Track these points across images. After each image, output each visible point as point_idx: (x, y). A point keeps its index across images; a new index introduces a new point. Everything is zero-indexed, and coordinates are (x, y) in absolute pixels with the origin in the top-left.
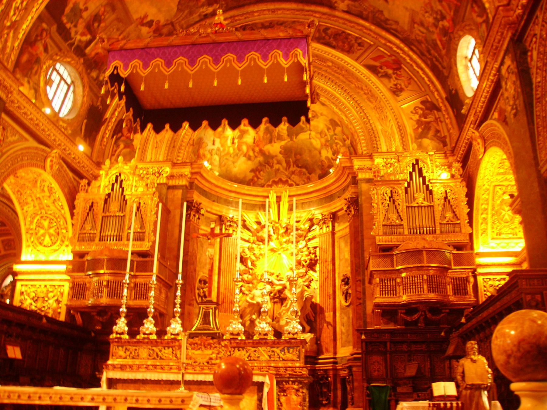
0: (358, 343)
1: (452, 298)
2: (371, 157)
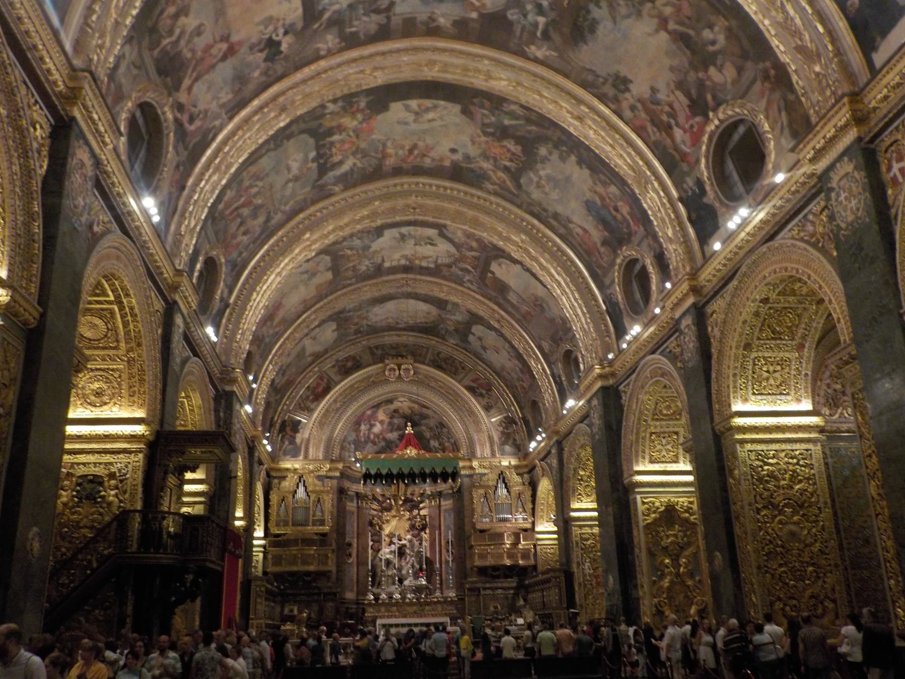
0: (460, 587)
1: (521, 562)
2: (470, 460)
